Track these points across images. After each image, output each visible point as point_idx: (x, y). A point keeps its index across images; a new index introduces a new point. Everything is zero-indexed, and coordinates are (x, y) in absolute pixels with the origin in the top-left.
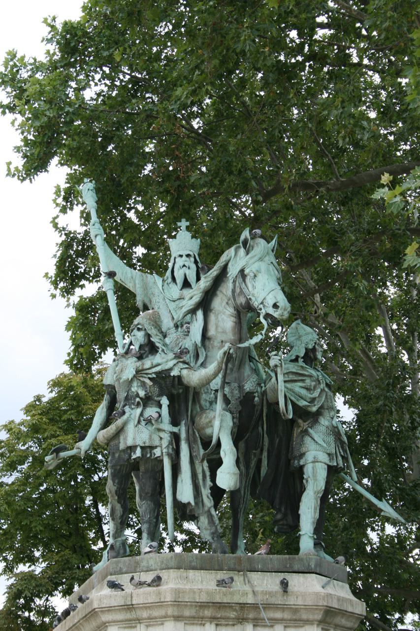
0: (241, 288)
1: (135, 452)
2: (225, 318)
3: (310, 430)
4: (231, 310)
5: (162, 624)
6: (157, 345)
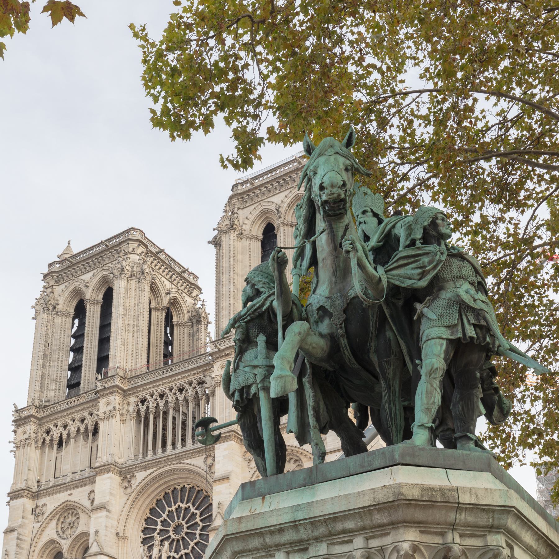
3: (425, 310)
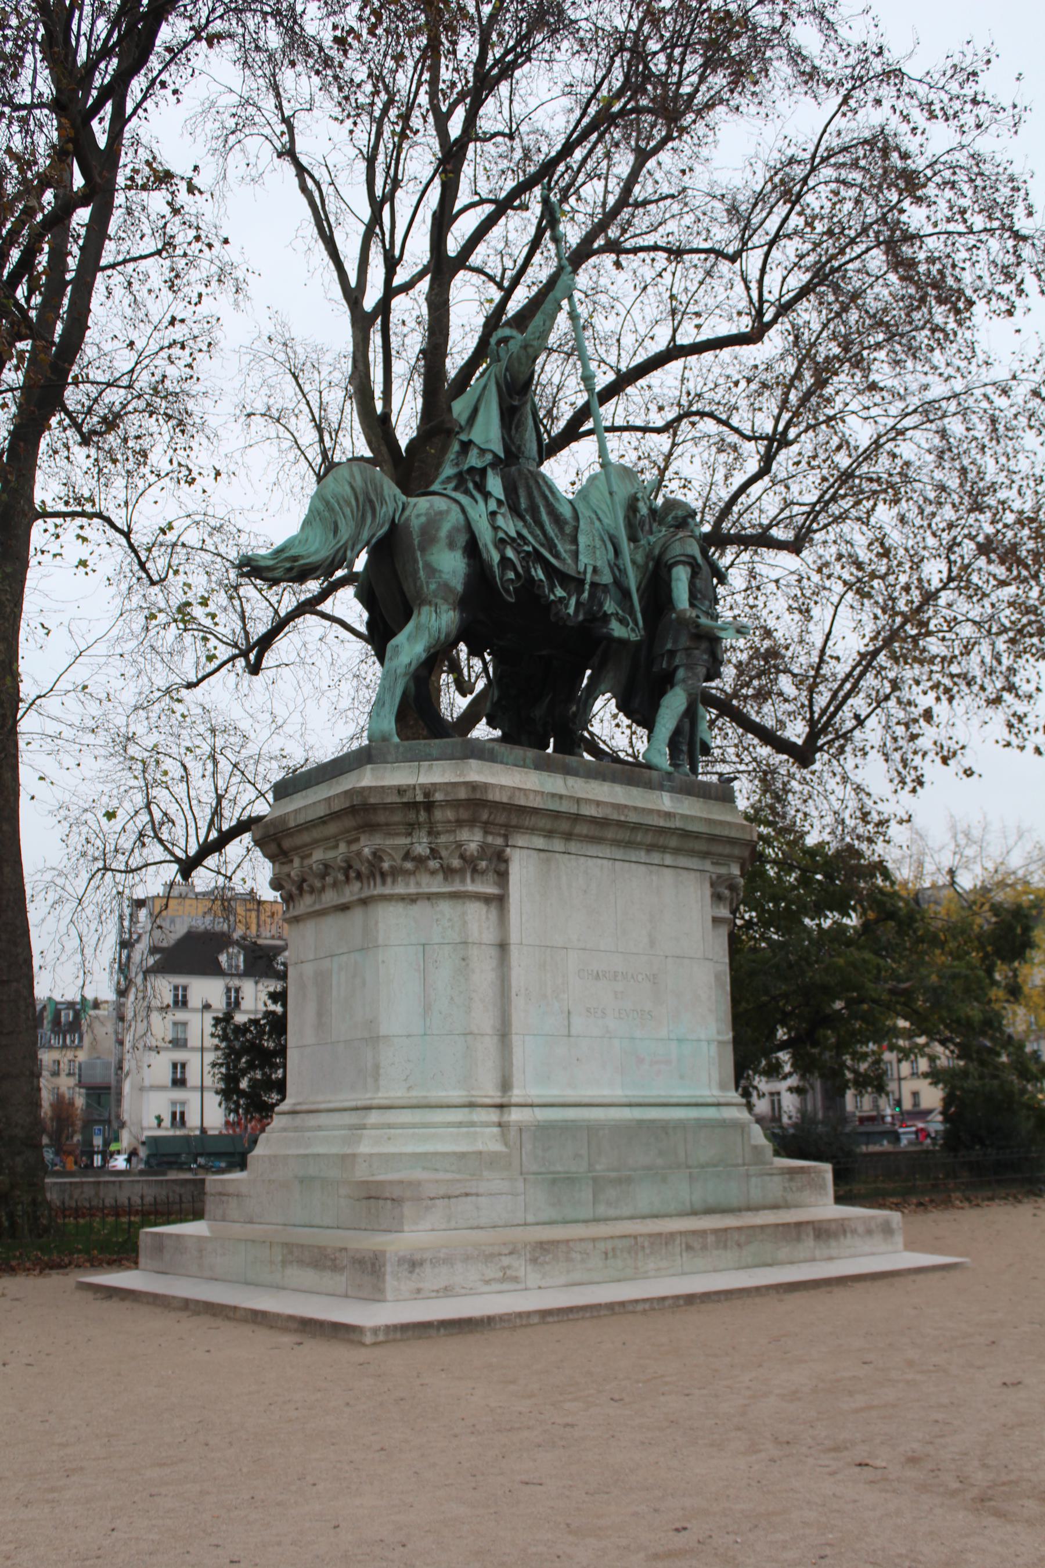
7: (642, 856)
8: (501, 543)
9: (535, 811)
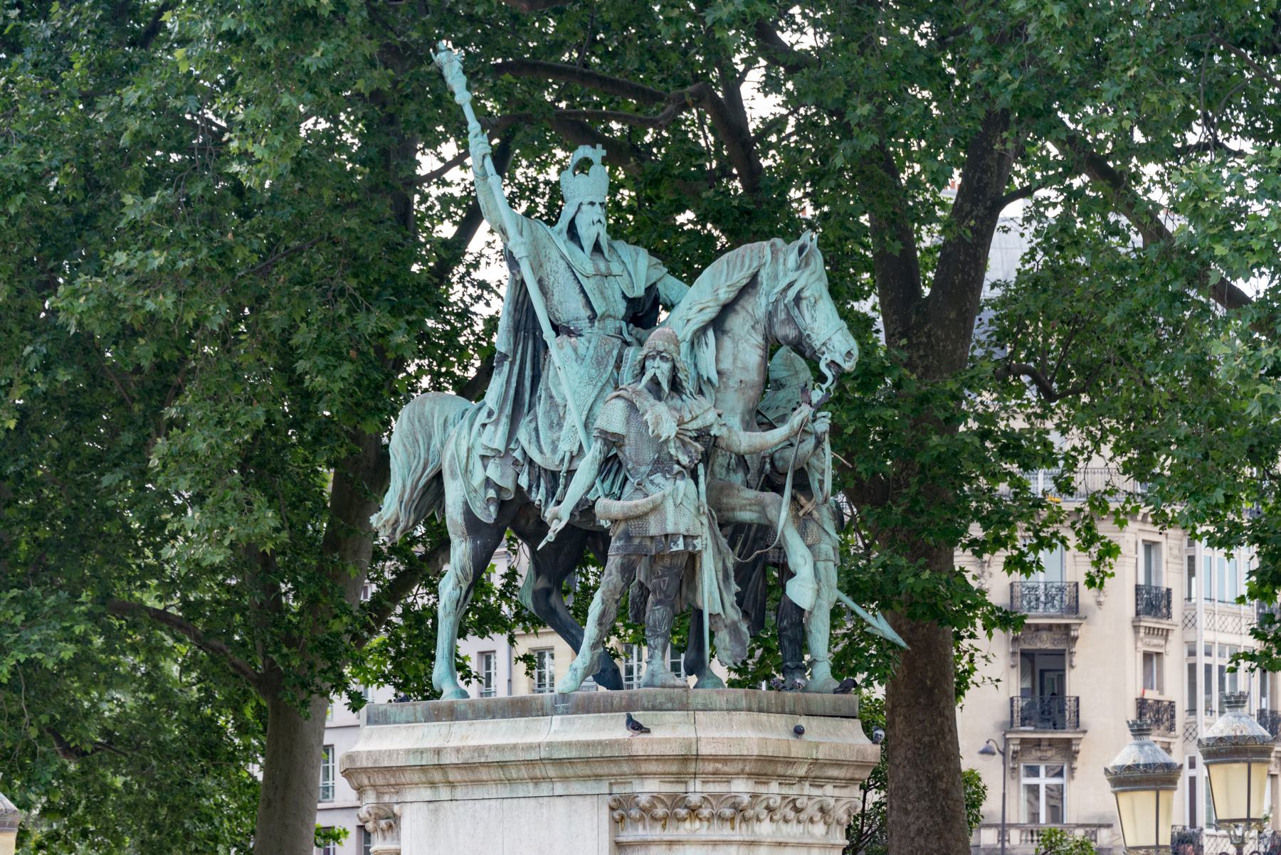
0: (788, 313)
1: (675, 543)
2: (748, 348)
4: (759, 339)
5: (728, 782)
6: (684, 384)
7: (531, 789)
8: (483, 457)
9: (401, 769)
